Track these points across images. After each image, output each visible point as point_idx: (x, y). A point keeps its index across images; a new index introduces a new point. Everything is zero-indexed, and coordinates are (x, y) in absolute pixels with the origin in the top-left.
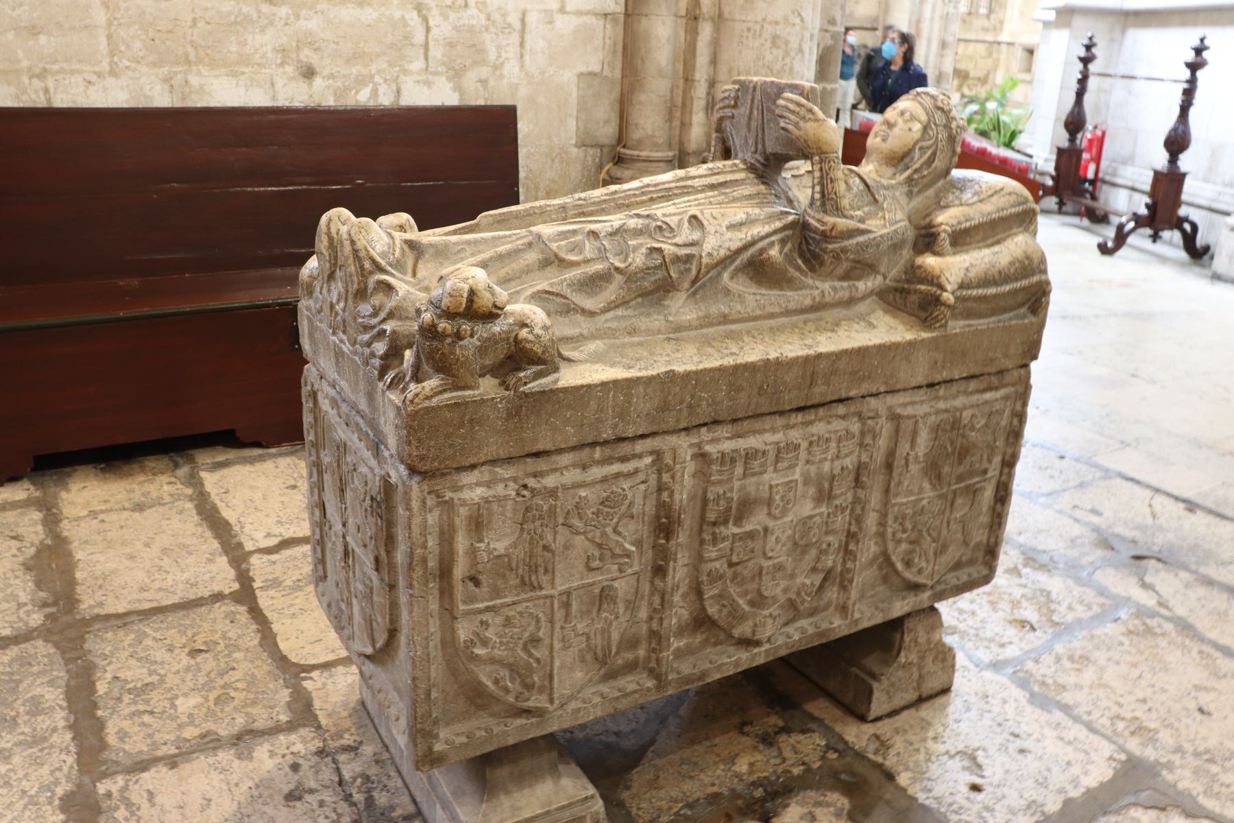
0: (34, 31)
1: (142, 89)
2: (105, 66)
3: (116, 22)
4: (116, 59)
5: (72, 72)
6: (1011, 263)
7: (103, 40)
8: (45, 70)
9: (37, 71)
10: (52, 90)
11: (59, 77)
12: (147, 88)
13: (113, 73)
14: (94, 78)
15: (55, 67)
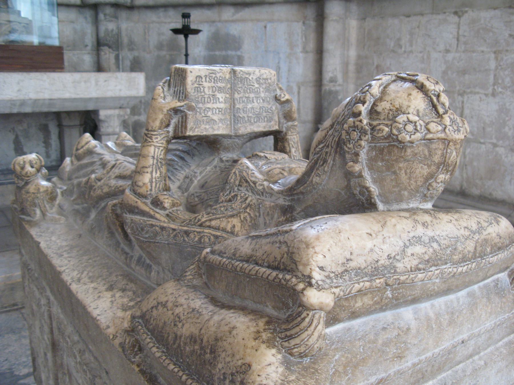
0: (464, 72)
1: (505, 105)
2: (490, 90)
3: (500, 68)
4: (496, 87)
5: (475, 93)
6: (193, 339)
7: (492, 77)
8: (464, 92)
9: (461, 92)
10: (465, 102)
11: (470, 95)
12: (508, 104)
13: (494, 95)
14: (484, 97)
15: (469, 91)
